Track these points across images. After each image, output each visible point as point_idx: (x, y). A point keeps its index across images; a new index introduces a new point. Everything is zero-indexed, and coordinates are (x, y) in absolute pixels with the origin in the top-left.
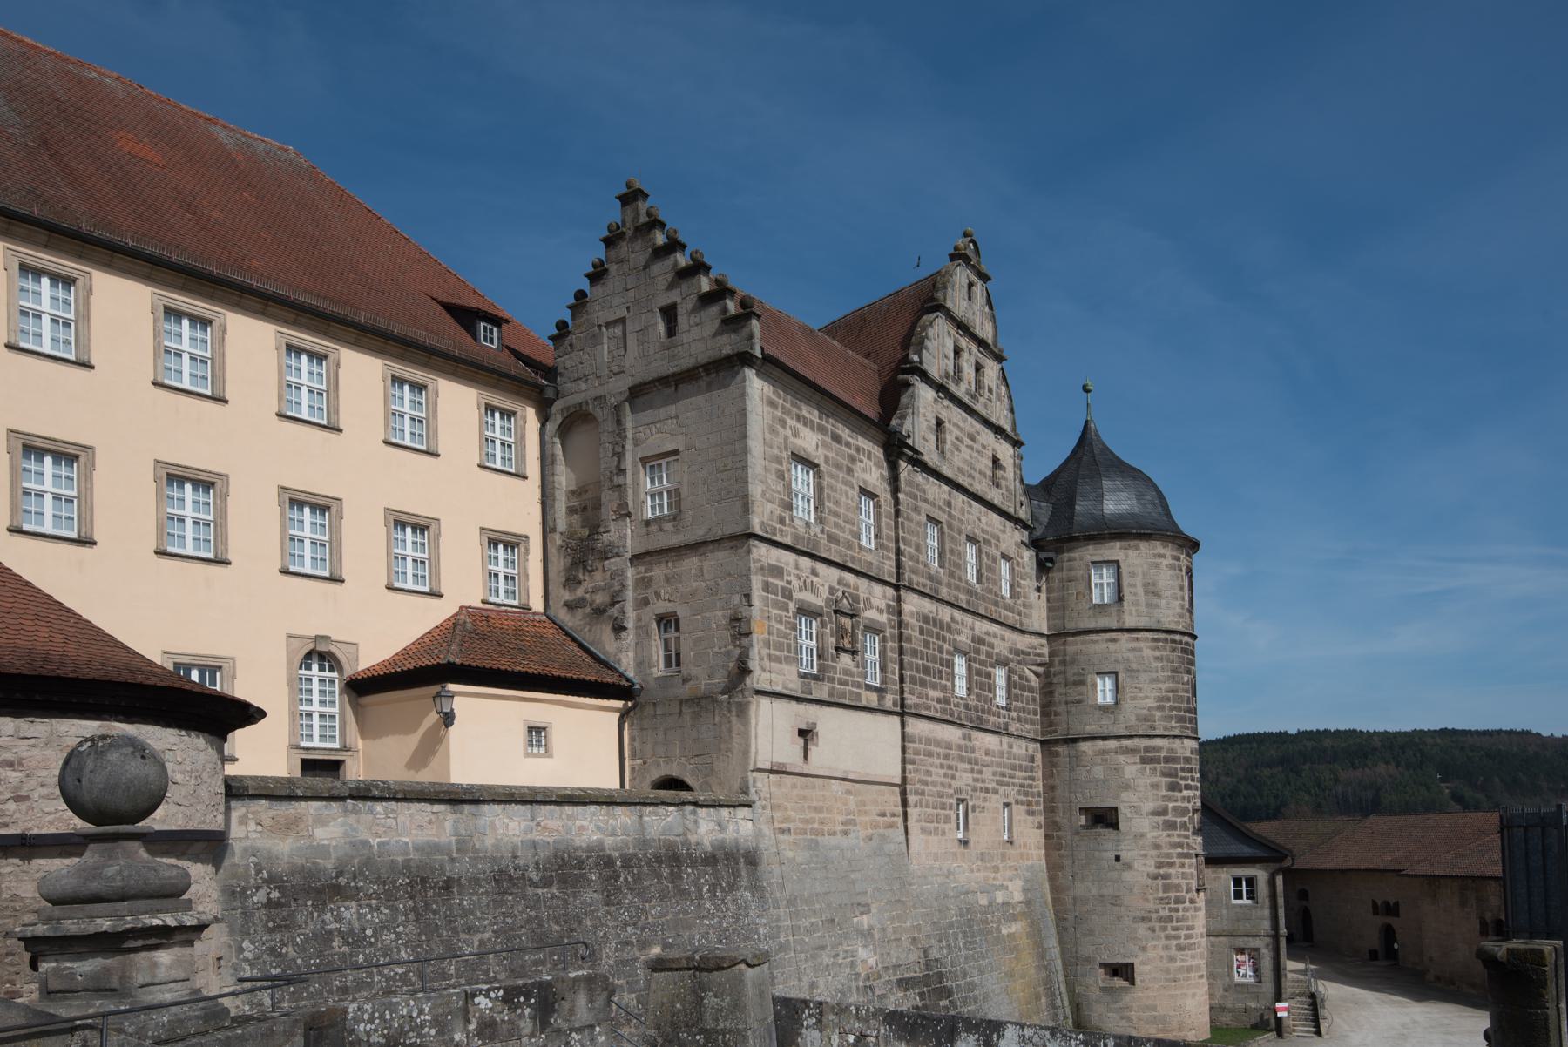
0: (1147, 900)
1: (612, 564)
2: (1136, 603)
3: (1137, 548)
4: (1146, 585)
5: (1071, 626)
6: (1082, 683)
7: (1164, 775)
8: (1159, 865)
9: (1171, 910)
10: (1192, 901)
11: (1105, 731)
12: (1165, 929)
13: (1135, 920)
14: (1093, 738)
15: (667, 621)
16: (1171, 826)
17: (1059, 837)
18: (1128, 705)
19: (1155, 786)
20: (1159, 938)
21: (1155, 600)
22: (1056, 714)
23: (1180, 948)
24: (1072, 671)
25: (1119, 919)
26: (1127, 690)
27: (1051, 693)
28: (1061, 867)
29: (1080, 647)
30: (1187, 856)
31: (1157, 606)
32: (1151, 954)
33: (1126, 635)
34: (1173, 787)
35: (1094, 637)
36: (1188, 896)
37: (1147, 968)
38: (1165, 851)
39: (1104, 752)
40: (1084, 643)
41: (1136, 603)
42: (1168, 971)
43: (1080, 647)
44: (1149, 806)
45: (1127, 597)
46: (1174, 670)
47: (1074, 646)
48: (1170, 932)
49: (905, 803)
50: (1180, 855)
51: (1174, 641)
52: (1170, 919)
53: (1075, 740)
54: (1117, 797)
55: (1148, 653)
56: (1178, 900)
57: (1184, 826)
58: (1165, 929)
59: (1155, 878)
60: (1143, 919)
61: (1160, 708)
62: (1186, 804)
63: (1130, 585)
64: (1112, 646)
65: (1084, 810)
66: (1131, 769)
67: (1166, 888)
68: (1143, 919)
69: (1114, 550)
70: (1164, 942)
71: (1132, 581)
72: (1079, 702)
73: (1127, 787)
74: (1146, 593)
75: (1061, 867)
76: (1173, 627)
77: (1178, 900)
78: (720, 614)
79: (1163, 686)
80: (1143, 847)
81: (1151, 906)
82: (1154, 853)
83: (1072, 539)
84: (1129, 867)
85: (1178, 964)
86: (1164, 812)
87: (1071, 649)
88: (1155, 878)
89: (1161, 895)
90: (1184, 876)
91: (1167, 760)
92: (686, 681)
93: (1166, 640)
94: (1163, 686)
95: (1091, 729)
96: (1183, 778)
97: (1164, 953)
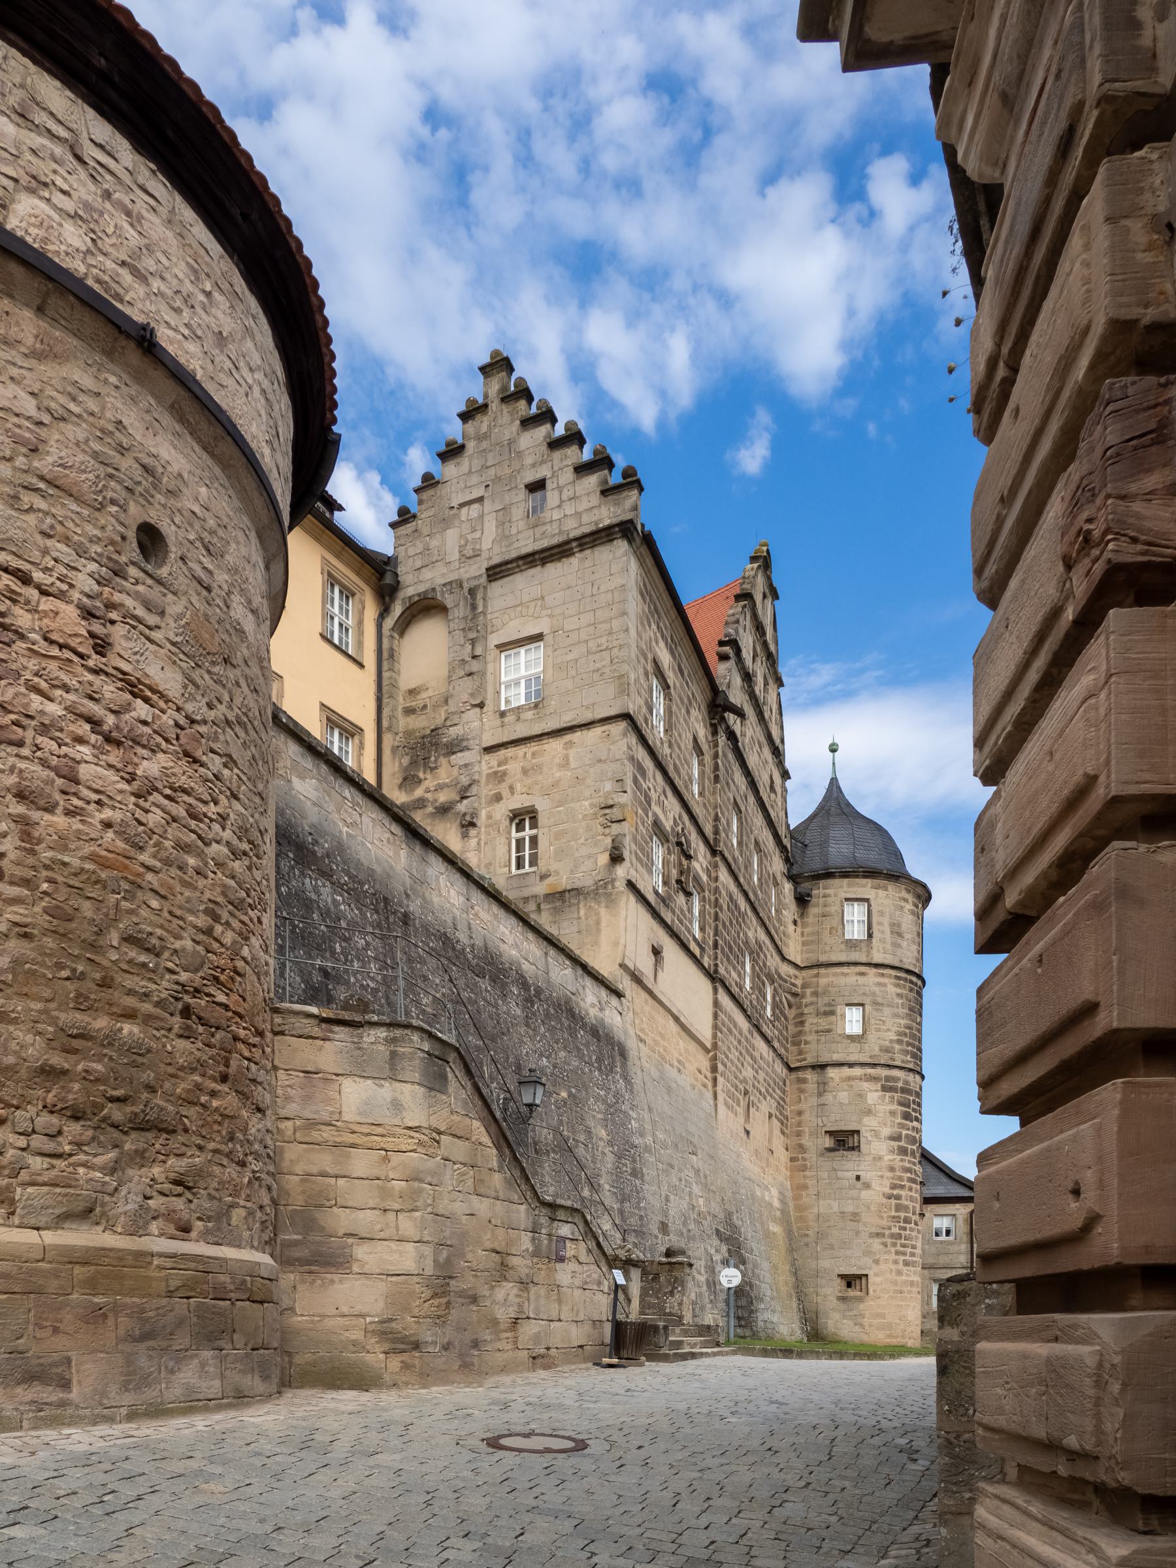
0: (882, 1218)
1: (459, 758)
2: (883, 941)
3: (886, 889)
4: (892, 925)
5: (823, 958)
6: (832, 1013)
7: (901, 1104)
8: (893, 1187)
9: (901, 1228)
10: (916, 1224)
11: (853, 1058)
13: (872, 1235)
14: (841, 1065)
15: (524, 817)
16: (903, 1151)
17: (804, 1159)
18: (872, 1037)
19: (893, 1113)
21: (900, 941)
22: (806, 1043)
23: (906, 1264)
24: (822, 1002)
25: (858, 1233)
26: (872, 1021)
27: (802, 1023)
28: (805, 1187)
29: (831, 979)
30: (913, 1181)
31: (900, 946)
32: (883, 1267)
33: (874, 970)
35: (845, 970)
36: (914, 1218)
37: (879, 1279)
38: (898, 1174)
39: (850, 1078)
40: (835, 975)
41: (883, 941)
42: (895, 1283)
43: (831, 979)
44: (886, 1131)
45: (876, 934)
46: (911, 1009)
47: (827, 978)
49: (714, 1069)
51: (911, 982)
52: (899, 1236)
53: (823, 1067)
54: (860, 1122)
55: (892, 990)
56: (907, 1220)
58: (894, 1245)
59: (889, 1198)
60: (878, 1235)
61: (899, 1042)
62: (914, 1134)
63: (880, 924)
64: (861, 980)
65: (830, 1133)
66: (873, 1095)
67: (898, 1208)
68: (878, 1235)
69: (864, 888)
70: (894, 1257)
71: (881, 919)
72: (829, 1031)
73: (869, 1112)
74: (892, 932)
75: (805, 1187)
76: (911, 968)
77: (907, 1220)
78: (587, 803)
80: (880, 1169)
81: (885, 1223)
82: (890, 1174)
83: (829, 875)
84: (867, 1186)
85: (904, 1278)
86: (897, 1138)
87: (823, 981)
88: (889, 1197)
89: (893, 1213)
90: (912, 1199)
91: (903, 1090)
92: (543, 877)
93: (906, 980)
94: (903, 1022)
95: (836, 1057)
96: (914, 1110)
97: (893, 1267)
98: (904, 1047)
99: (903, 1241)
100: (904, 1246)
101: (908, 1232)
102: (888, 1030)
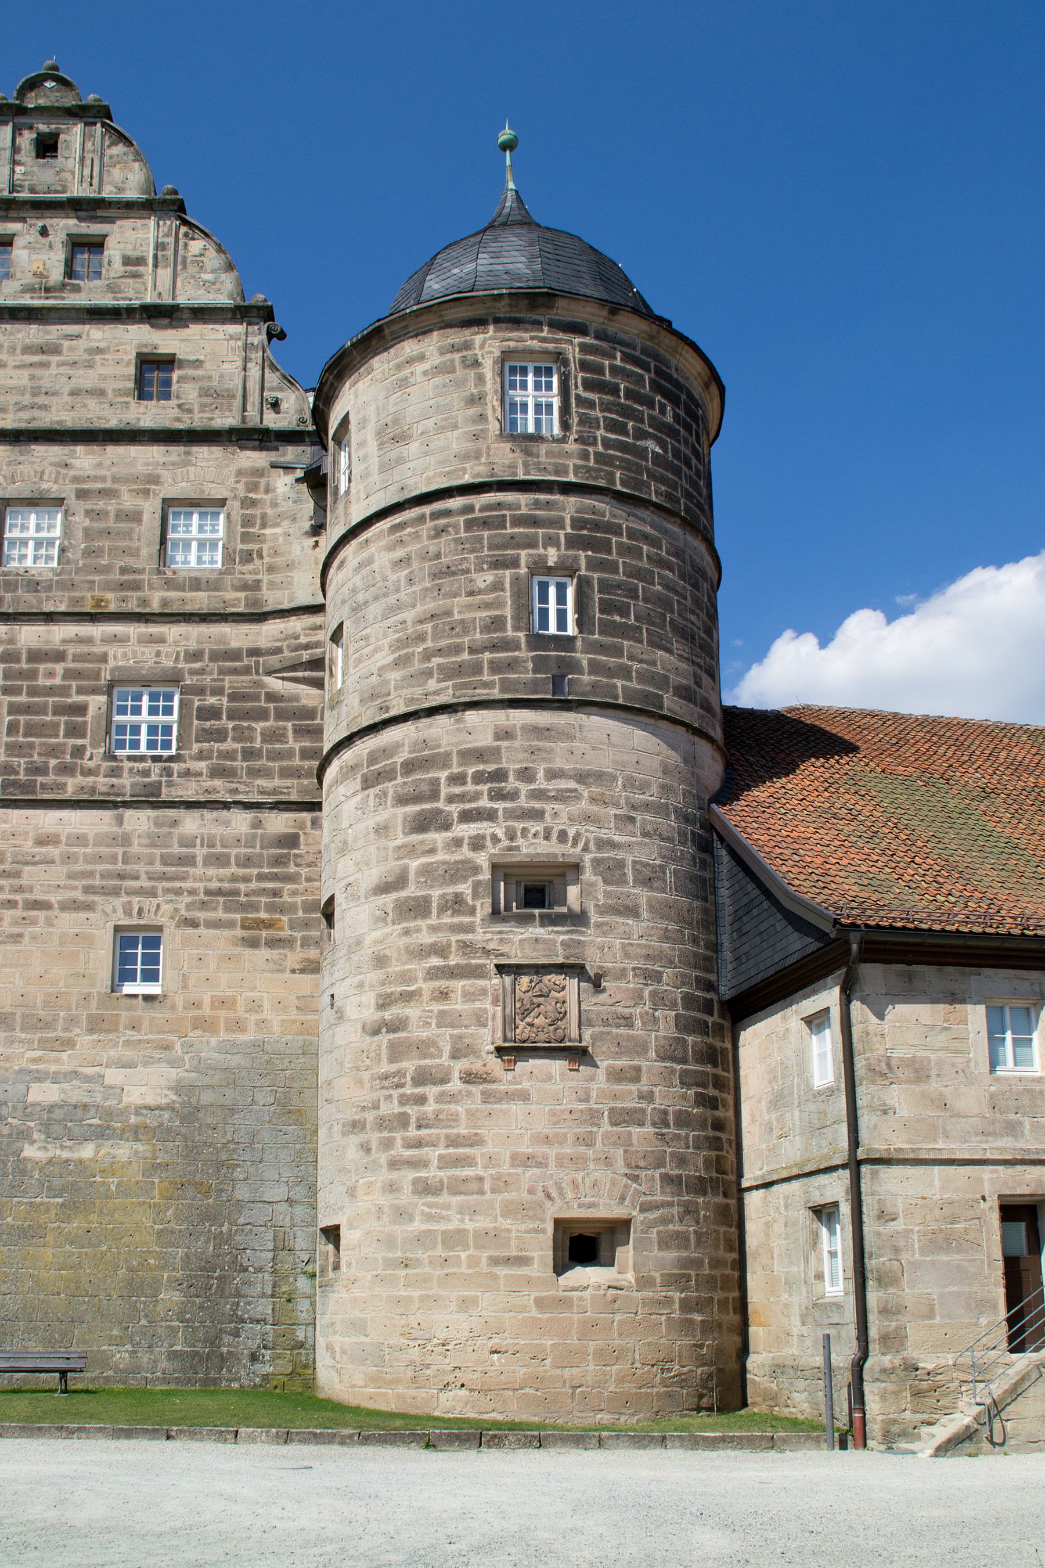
7: (402, 800)
9: (404, 1100)
12: (387, 1144)
16: (418, 908)
19: (383, 830)
20: (376, 1164)
23: (424, 1188)
34: (422, 824)
44: (373, 875)
48: (400, 1151)
50: (433, 974)
57: (457, 904)
58: (387, 1144)
59: (376, 1032)
70: (386, 1175)
79: (409, 615)
86: (400, 881)
89: (386, 1067)
91: (409, 767)
94: (409, 615)
98: (417, 666)
99: (412, 1132)
100: (419, 1144)
101: (430, 1108)
102: (377, 650)
